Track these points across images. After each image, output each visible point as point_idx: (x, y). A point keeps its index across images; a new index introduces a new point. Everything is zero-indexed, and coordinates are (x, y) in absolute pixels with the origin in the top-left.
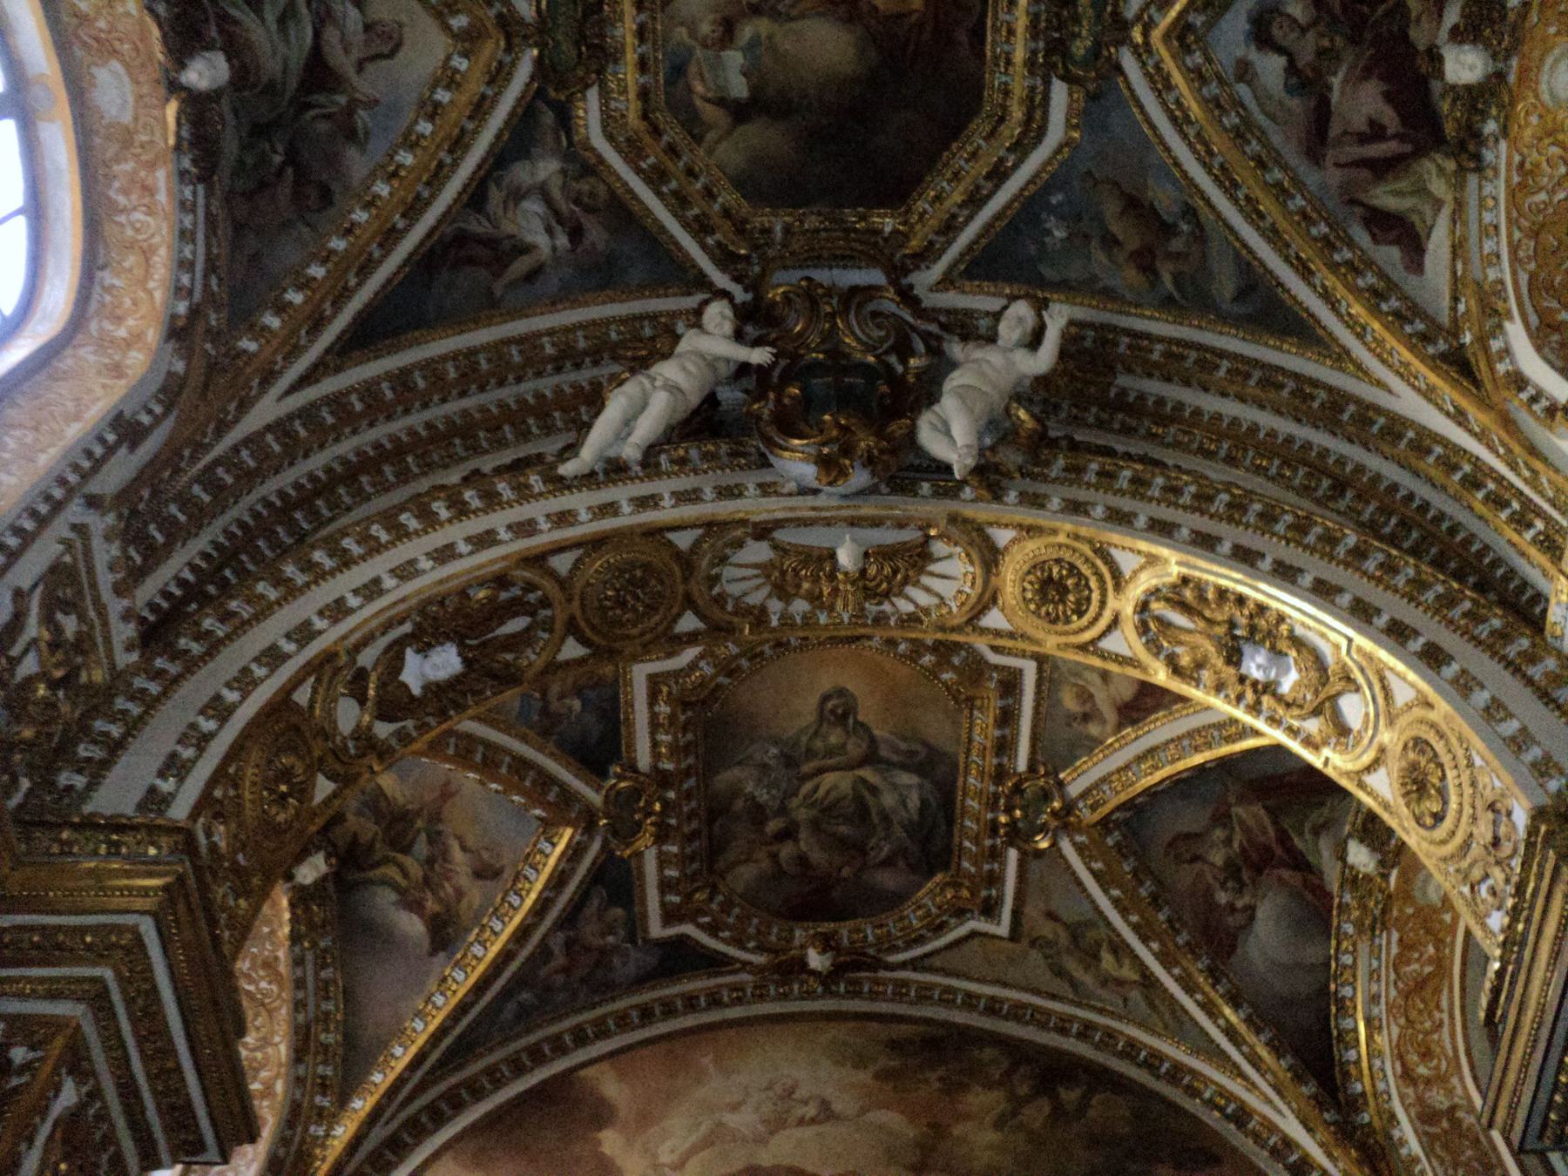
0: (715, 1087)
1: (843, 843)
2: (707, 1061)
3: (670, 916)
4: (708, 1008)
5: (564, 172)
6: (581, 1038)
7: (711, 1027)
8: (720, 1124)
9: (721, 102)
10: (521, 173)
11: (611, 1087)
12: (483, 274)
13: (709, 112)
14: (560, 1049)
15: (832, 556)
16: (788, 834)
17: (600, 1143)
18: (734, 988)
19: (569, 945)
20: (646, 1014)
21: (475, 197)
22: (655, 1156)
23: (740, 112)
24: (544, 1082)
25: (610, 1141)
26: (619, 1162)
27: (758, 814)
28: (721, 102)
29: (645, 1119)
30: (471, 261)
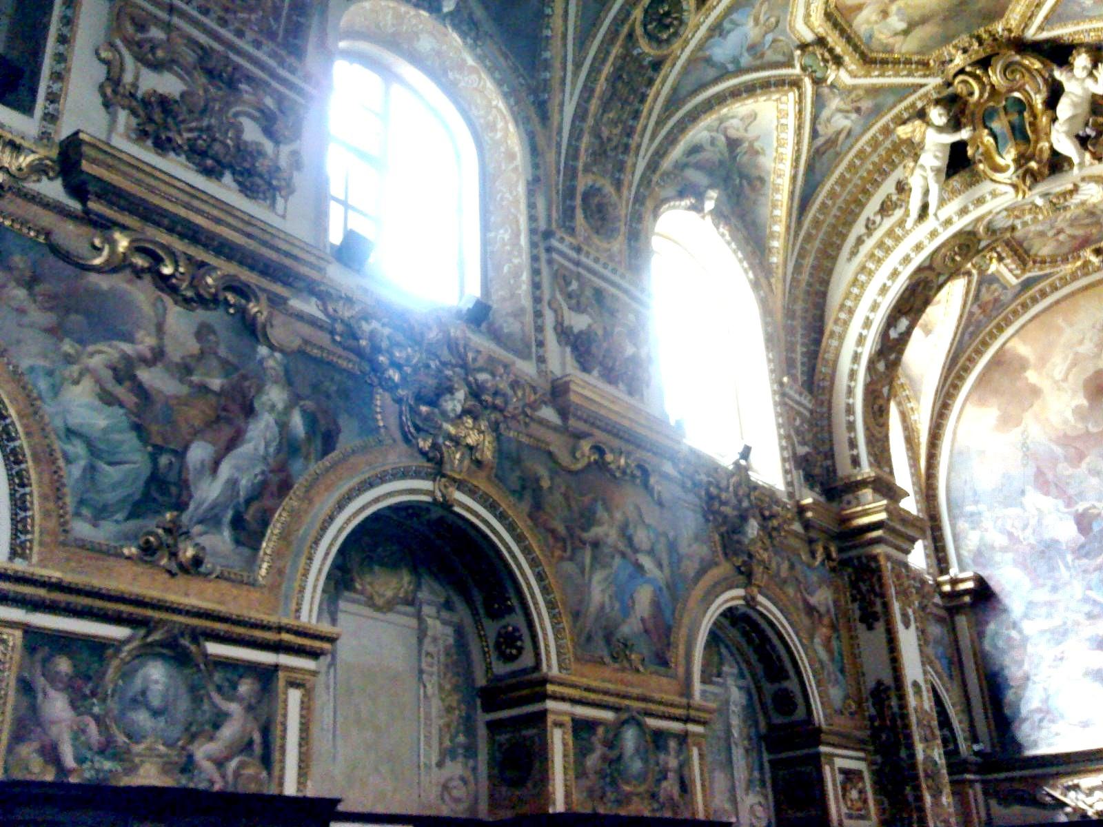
0: (1069, 334)
1: (1088, 225)
2: (1060, 321)
3: (1017, 277)
4: (1052, 292)
5: (842, 99)
6: (1000, 329)
7: (1057, 302)
8: (1076, 354)
9: (896, 34)
10: (825, 114)
11: (1021, 348)
12: (832, 151)
13: (891, 40)
14: (993, 336)
15: (1037, 206)
16: (1060, 232)
17: (1027, 379)
18: (1061, 279)
19: (980, 307)
20: (1025, 307)
21: (815, 134)
22: (1052, 378)
23: (906, 32)
24: (993, 357)
25: (1031, 376)
26: (1039, 385)
27: (1042, 234)
28: (896, 34)
29: (1043, 360)
30: (824, 153)
